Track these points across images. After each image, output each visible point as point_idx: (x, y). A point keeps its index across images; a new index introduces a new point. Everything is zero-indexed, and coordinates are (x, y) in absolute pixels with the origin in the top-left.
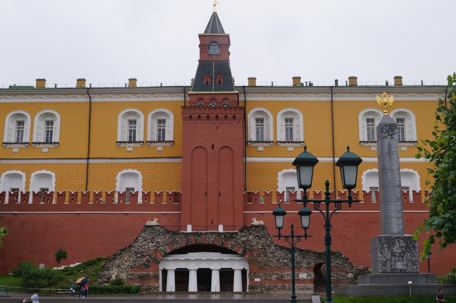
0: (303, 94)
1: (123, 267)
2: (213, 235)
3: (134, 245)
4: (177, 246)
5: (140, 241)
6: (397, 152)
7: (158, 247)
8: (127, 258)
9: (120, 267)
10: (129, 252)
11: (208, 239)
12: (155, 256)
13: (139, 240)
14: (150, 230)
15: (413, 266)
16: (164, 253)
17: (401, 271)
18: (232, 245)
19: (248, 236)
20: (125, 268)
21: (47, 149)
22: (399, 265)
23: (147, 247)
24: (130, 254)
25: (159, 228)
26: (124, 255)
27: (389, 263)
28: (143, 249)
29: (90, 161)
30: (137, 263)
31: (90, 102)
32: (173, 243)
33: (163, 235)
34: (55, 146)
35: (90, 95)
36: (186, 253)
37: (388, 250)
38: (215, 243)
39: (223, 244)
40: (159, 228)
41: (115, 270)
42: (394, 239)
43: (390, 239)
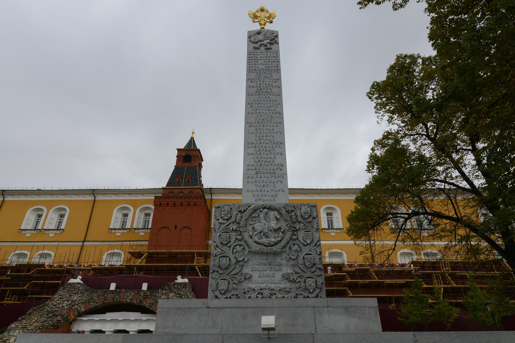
1: (30, 329)
2: (133, 292)
3: (48, 303)
4: (93, 305)
5: (56, 299)
6: (276, 67)
7: (73, 306)
8: (37, 318)
9: (26, 328)
10: (42, 311)
11: (127, 297)
12: (67, 316)
13: (55, 298)
14: (70, 288)
15: (307, 281)
16: (77, 313)
17: (271, 294)
18: (150, 304)
19: (169, 293)
20: (31, 330)
22: (268, 279)
23: (61, 305)
24: (41, 314)
25: (79, 286)
26: (35, 315)
27: (238, 273)
28: (56, 308)
30: (46, 324)
32: (89, 302)
33: (81, 293)
36: (104, 313)
37: (239, 237)
38: (132, 301)
39: (141, 303)
40: (79, 286)
41: (19, 332)
42: (255, 210)
43: (245, 211)
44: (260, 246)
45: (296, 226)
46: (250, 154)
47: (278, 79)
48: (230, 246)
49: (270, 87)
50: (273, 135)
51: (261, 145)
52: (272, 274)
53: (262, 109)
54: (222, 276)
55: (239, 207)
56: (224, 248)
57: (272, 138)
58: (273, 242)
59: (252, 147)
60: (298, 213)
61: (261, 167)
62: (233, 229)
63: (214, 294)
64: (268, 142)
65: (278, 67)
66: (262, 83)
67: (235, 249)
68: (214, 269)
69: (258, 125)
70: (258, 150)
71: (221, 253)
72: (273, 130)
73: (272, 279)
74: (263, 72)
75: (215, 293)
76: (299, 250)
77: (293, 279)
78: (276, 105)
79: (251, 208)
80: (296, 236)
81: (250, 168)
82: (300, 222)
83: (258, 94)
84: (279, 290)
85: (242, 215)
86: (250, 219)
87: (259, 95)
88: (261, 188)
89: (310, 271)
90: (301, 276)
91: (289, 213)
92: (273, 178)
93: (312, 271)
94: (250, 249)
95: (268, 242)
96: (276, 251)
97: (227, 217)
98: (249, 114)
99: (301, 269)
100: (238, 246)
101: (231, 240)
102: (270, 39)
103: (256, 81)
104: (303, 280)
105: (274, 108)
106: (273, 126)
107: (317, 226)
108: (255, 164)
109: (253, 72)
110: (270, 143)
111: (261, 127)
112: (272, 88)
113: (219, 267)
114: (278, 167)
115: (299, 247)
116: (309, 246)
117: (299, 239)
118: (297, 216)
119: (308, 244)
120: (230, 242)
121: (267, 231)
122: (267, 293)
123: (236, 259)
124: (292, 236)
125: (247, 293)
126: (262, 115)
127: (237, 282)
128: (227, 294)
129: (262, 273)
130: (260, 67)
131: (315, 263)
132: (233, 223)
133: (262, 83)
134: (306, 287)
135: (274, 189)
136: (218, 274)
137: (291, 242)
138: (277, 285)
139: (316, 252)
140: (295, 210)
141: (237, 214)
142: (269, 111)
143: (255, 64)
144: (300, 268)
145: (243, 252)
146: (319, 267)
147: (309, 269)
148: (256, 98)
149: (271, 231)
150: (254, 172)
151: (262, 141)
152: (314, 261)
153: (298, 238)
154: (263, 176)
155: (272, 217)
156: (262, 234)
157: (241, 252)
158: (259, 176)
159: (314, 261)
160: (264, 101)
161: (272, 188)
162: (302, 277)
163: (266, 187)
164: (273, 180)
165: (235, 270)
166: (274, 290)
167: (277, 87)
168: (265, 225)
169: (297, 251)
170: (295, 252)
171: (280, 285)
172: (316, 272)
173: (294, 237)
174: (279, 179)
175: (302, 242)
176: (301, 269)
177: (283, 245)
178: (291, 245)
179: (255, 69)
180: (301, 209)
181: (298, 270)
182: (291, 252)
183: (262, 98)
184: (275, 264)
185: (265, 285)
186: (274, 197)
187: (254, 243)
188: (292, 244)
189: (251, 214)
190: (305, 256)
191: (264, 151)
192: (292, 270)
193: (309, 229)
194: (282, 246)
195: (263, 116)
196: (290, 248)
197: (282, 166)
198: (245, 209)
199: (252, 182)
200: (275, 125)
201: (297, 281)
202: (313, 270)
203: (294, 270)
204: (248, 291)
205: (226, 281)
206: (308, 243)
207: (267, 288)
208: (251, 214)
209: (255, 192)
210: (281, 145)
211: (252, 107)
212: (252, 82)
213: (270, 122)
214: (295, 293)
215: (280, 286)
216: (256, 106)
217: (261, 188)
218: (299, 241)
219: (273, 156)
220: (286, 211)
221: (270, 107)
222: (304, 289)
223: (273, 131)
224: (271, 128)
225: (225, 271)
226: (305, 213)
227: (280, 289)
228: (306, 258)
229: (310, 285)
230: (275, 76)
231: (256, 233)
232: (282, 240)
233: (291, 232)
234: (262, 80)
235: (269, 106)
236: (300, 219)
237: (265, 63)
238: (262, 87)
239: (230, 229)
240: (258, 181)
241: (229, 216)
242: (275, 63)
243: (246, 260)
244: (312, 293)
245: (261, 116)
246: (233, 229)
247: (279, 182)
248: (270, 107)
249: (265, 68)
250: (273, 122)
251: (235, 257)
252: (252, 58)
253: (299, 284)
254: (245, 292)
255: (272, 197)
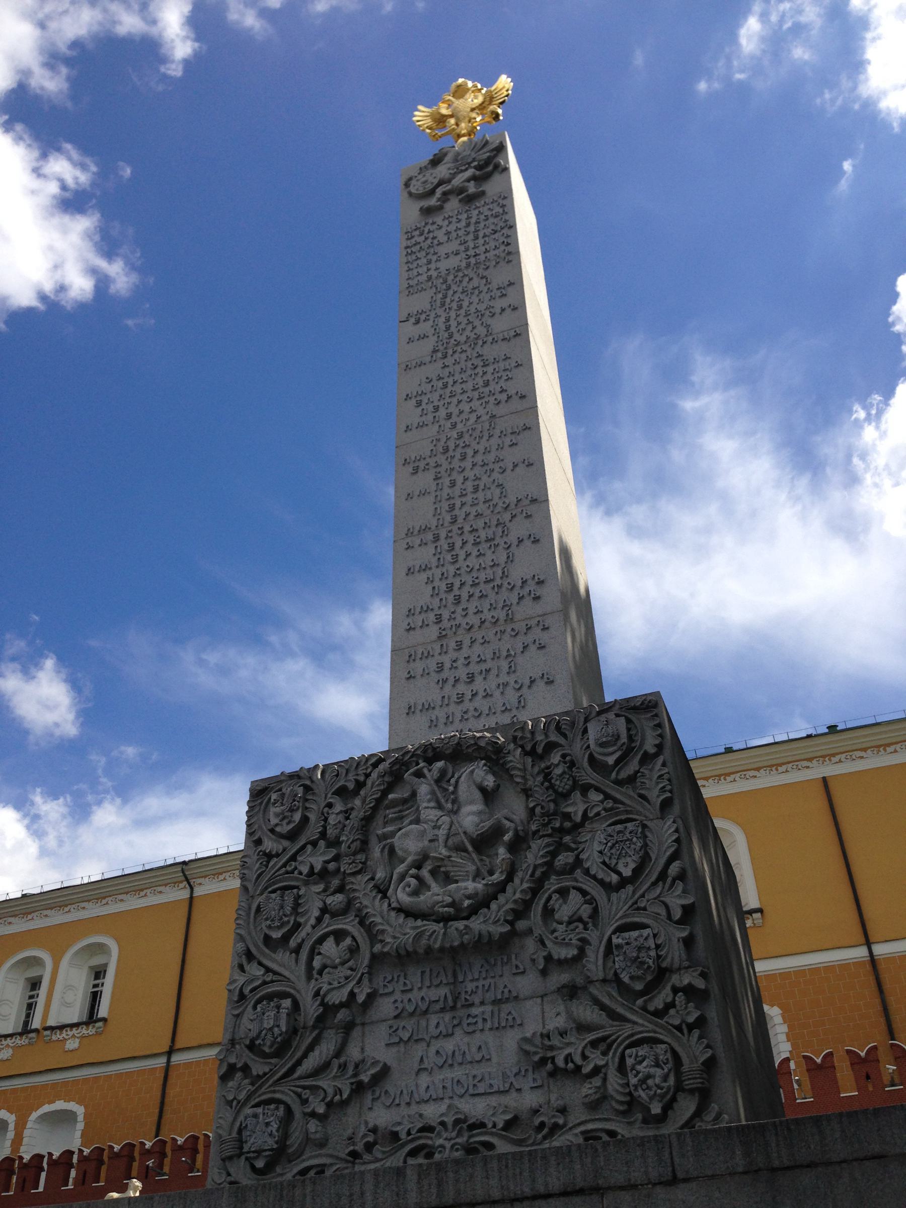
0: (733, 776)
6: (503, 247)
21: (76, 1039)
22: (458, 1073)
29: (176, 1058)
31: (191, 898)
34: (98, 1028)
35: (192, 881)
43: (360, 785)
44: (419, 922)
45: (570, 809)
46: (417, 568)
47: (511, 284)
48: (300, 946)
49: (484, 320)
50: (500, 478)
51: (455, 528)
52: (474, 1049)
53: (455, 400)
54: (263, 1090)
55: (337, 775)
56: (274, 960)
57: (498, 491)
58: (469, 897)
59: (423, 544)
60: (577, 750)
61: (459, 610)
62: (312, 867)
63: (229, 1174)
64: (481, 508)
65: (508, 244)
66: (453, 314)
67: (319, 954)
68: (232, 1060)
69: (441, 459)
70: (446, 547)
71: (265, 983)
72: (498, 460)
73: (478, 1071)
74: (458, 279)
75: (232, 1171)
76: (585, 916)
77: (568, 1058)
78: (504, 374)
79: (381, 767)
80: (572, 850)
81: (418, 620)
82: (585, 790)
83: (440, 355)
84: (509, 1125)
85: (350, 806)
86: (379, 819)
87: (445, 357)
88: (461, 688)
89: (644, 1008)
90: (604, 1039)
91: (541, 757)
92: (506, 637)
93: (651, 1008)
94: (378, 948)
95: (449, 900)
96: (484, 933)
97: (291, 826)
98: (409, 433)
99: (603, 1007)
100: (331, 941)
101: (302, 920)
102: (476, 163)
103: (433, 315)
104: (612, 1059)
105: (502, 383)
106: (500, 448)
107: (663, 790)
108: (436, 602)
109: (423, 290)
110: (489, 512)
111: (456, 463)
112: (489, 321)
113: (251, 1047)
114: (525, 592)
115: (586, 902)
116: (630, 888)
117: (586, 865)
118: (572, 764)
119: (624, 882)
120: (297, 926)
121: (444, 852)
122: (448, 1145)
123: (323, 1000)
124: (554, 854)
125: (367, 1157)
126: (458, 420)
127: (321, 1110)
128: (278, 1170)
129: (433, 1050)
130: (444, 265)
131: (664, 965)
132: (314, 844)
133: (453, 314)
134: (630, 1094)
135: (511, 679)
136: (247, 1081)
137: (553, 884)
138: (493, 1101)
139: (663, 912)
140: (562, 741)
141: (330, 805)
142: (483, 401)
143: (429, 262)
144: (596, 1002)
145: (350, 963)
146: (686, 982)
147: (640, 1002)
148: (433, 370)
149: (460, 848)
150: (433, 632)
151: (461, 514)
152: (659, 957)
153: (578, 862)
154: (466, 642)
155: (466, 790)
156: (425, 873)
157: (343, 963)
158: (452, 645)
159: (659, 957)
160: (462, 371)
161: (504, 678)
162: (609, 1047)
163: (479, 679)
164: (506, 644)
165: (316, 1052)
166: (482, 1125)
167: (508, 311)
168: (436, 827)
169: (580, 920)
170: (572, 926)
171: (511, 1100)
172: (672, 1012)
173: (565, 858)
174: (529, 639)
175: (600, 876)
176: (603, 1007)
177: (515, 901)
178: (550, 898)
179: (430, 278)
180: (585, 731)
181: (588, 1013)
182: (554, 931)
183: (456, 363)
184: (490, 996)
185: (443, 1108)
186: (514, 712)
187: (393, 914)
188: (556, 891)
189: (385, 793)
190: (615, 940)
191: (469, 547)
192: (563, 1014)
193: (627, 812)
194: (510, 906)
195: (460, 426)
196: (548, 913)
197: (540, 583)
198: (362, 778)
199: (425, 674)
200: (507, 441)
201: (587, 1070)
202: (658, 1003)
203: (570, 1016)
204: (369, 1147)
205: (272, 1106)
206: (627, 872)
207: (449, 1120)
208: (385, 793)
209: (436, 712)
210: (532, 509)
211: (419, 404)
212: (417, 322)
213: (486, 437)
214: (582, 1128)
215: (513, 1104)
216: (435, 397)
217: (461, 688)
218: (587, 872)
219: (503, 558)
220: (526, 753)
221: (487, 384)
222: (621, 1103)
223: (501, 464)
224: (491, 457)
225: (273, 1061)
226: (602, 745)
227: (508, 1117)
228: (619, 947)
229: (643, 1081)
230: (498, 277)
231: (401, 868)
232: (510, 878)
233: (547, 840)
234: (454, 305)
235: (481, 383)
236: (588, 776)
237: (462, 248)
238: (453, 329)
239: (300, 873)
240: (447, 665)
241: (297, 817)
242: (496, 236)
243: (361, 998)
244: (662, 1118)
245: (454, 426)
246: (312, 867)
247: (533, 648)
248: (487, 384)
249: (464, 264)
250: (497, 432)
251: (317, 994)
252: (418, 247)
253: (597, 1081)
254: (354, 1155)
255: (507, 714)
